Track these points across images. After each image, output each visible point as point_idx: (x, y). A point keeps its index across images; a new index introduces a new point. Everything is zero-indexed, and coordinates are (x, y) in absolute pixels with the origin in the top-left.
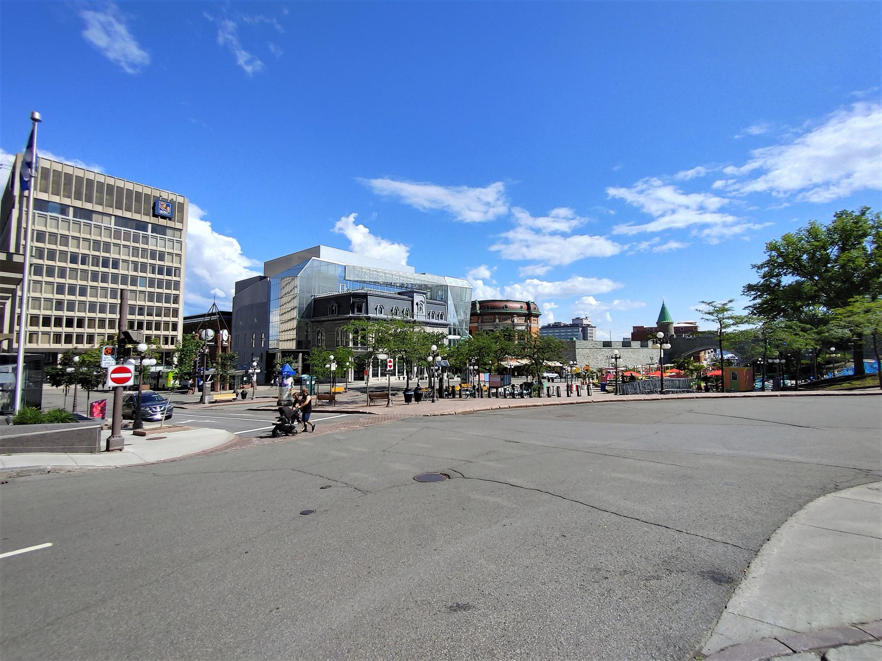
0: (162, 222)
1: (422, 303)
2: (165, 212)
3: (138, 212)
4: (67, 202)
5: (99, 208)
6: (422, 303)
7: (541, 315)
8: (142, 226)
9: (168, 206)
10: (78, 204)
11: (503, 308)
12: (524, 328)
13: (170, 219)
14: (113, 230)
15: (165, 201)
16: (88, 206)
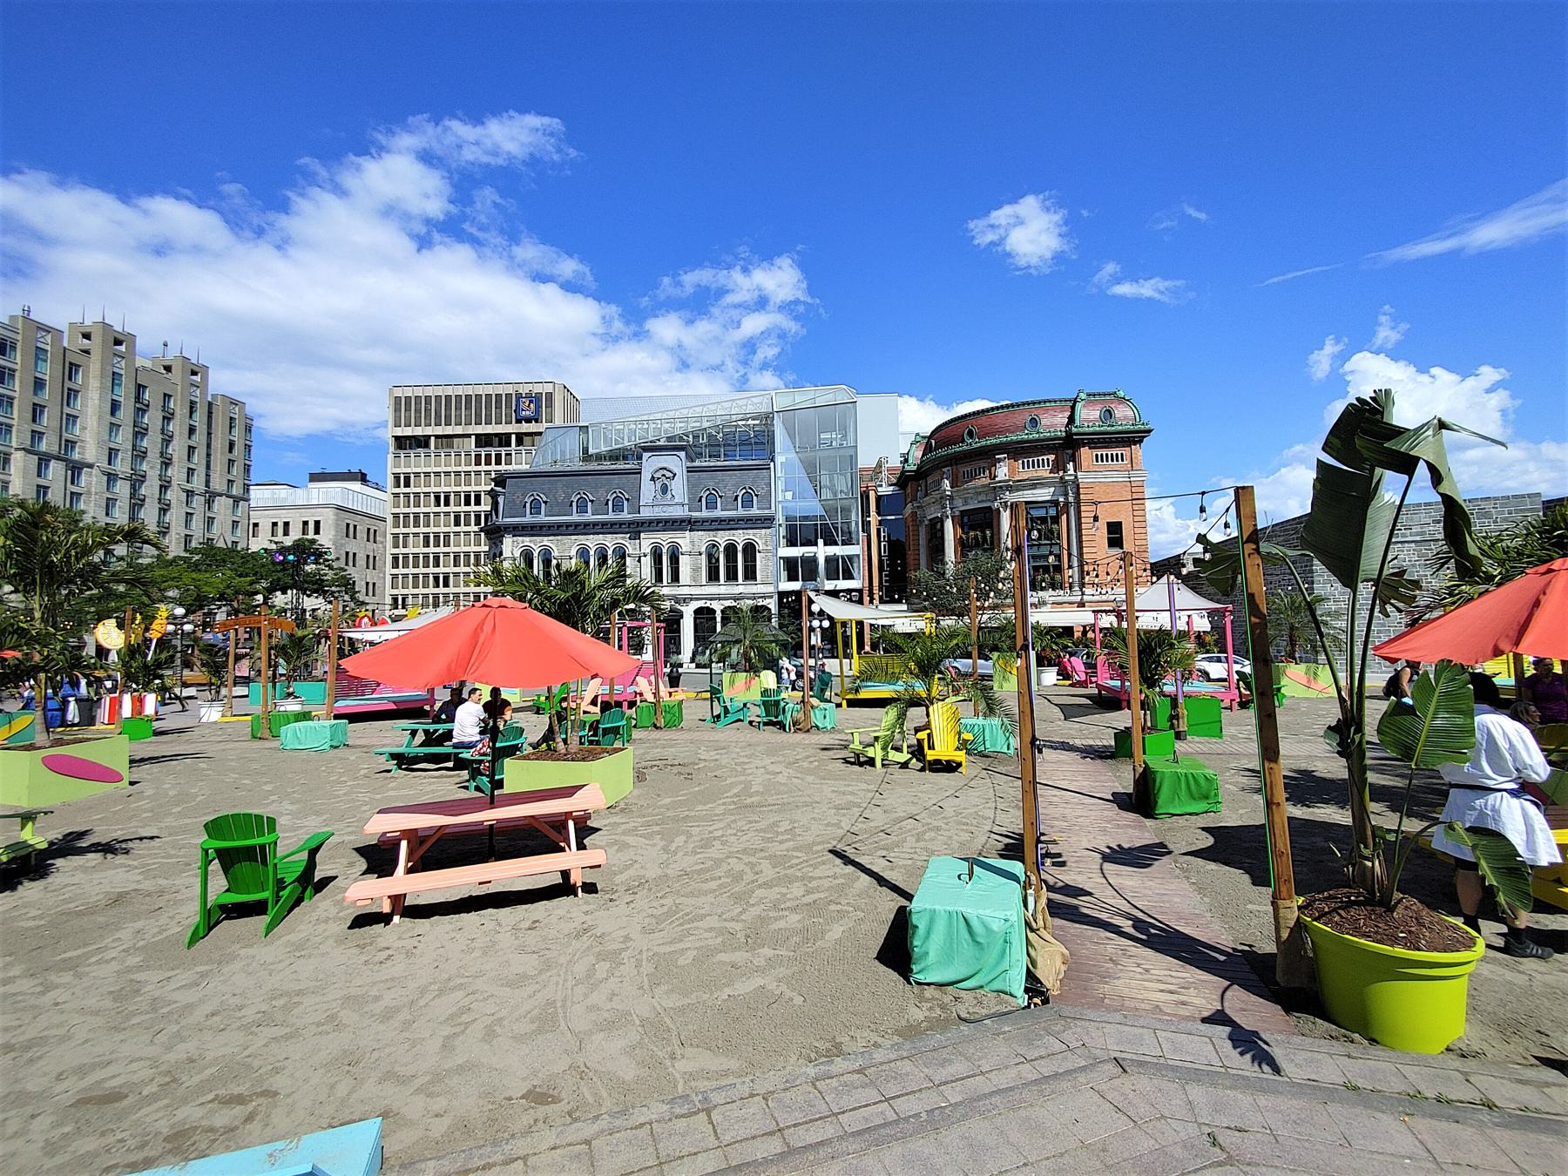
0: (525, 427)
1: (669, 474)
2: (528, 413)
3: (499, 422)
4: (429, 431)
5: (459, 430)
6: (669, 474)
7: (1149, 431)
8: (504, 440)
9: (531, 402)
10: (440, 431)
11: (963, 441)
12: (1044, 494)
13: (537, 421)
14: (473, 454)
15: (529, 396)
16: (449, 430)
